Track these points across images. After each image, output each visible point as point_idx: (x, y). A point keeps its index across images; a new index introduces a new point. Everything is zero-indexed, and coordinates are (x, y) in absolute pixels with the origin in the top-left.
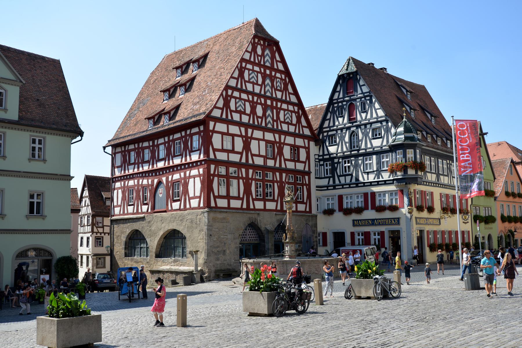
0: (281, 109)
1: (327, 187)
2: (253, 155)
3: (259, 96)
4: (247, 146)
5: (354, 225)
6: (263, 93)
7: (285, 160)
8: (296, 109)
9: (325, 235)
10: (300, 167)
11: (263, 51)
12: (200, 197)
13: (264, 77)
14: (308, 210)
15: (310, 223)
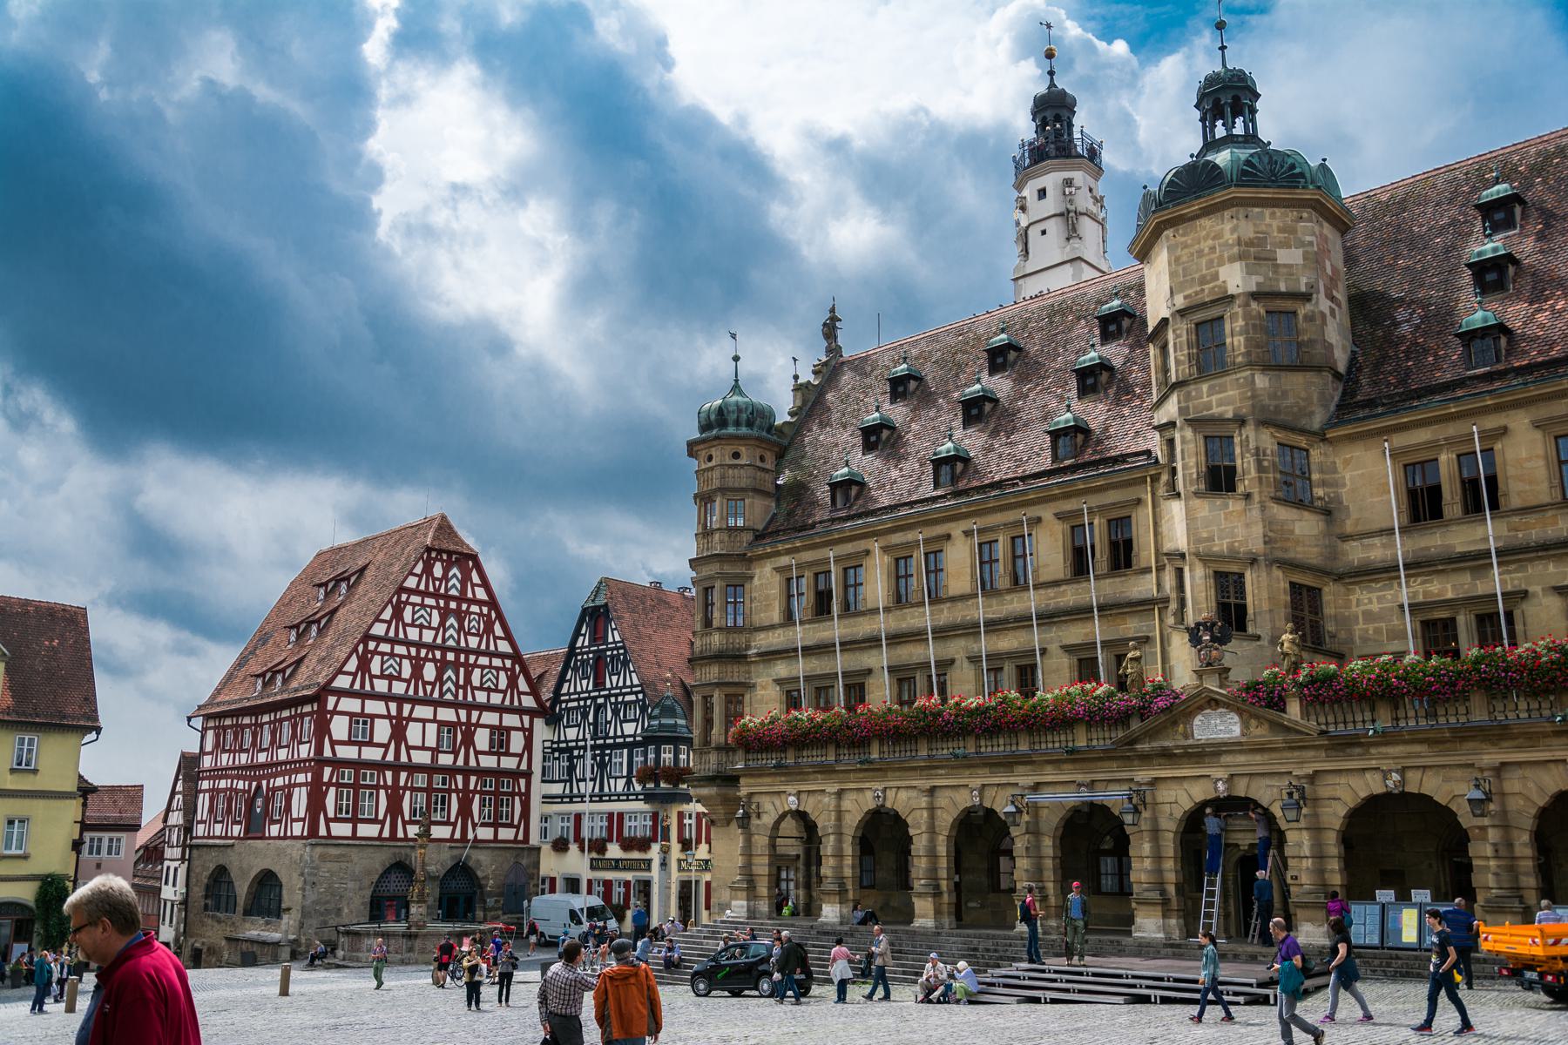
0: (475, 665)
1: (561, 798)
2: (409, 748)
3: (431, 647)
4: (398, 734)
5: (592, 868)
6: (439, 641)
7: (477, 753)
8: (508, 663)
9: (553, 880)
10: (509, 763)
11: (446, 571)
12: (303, 820)
13: (445, 614)
14: (520, 837)
15: (524, 862)
